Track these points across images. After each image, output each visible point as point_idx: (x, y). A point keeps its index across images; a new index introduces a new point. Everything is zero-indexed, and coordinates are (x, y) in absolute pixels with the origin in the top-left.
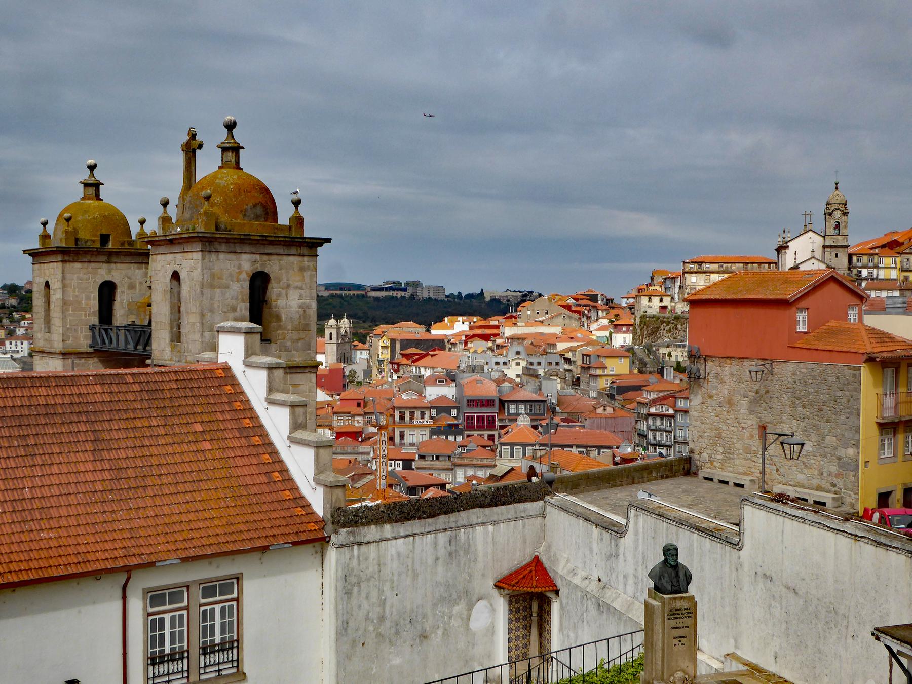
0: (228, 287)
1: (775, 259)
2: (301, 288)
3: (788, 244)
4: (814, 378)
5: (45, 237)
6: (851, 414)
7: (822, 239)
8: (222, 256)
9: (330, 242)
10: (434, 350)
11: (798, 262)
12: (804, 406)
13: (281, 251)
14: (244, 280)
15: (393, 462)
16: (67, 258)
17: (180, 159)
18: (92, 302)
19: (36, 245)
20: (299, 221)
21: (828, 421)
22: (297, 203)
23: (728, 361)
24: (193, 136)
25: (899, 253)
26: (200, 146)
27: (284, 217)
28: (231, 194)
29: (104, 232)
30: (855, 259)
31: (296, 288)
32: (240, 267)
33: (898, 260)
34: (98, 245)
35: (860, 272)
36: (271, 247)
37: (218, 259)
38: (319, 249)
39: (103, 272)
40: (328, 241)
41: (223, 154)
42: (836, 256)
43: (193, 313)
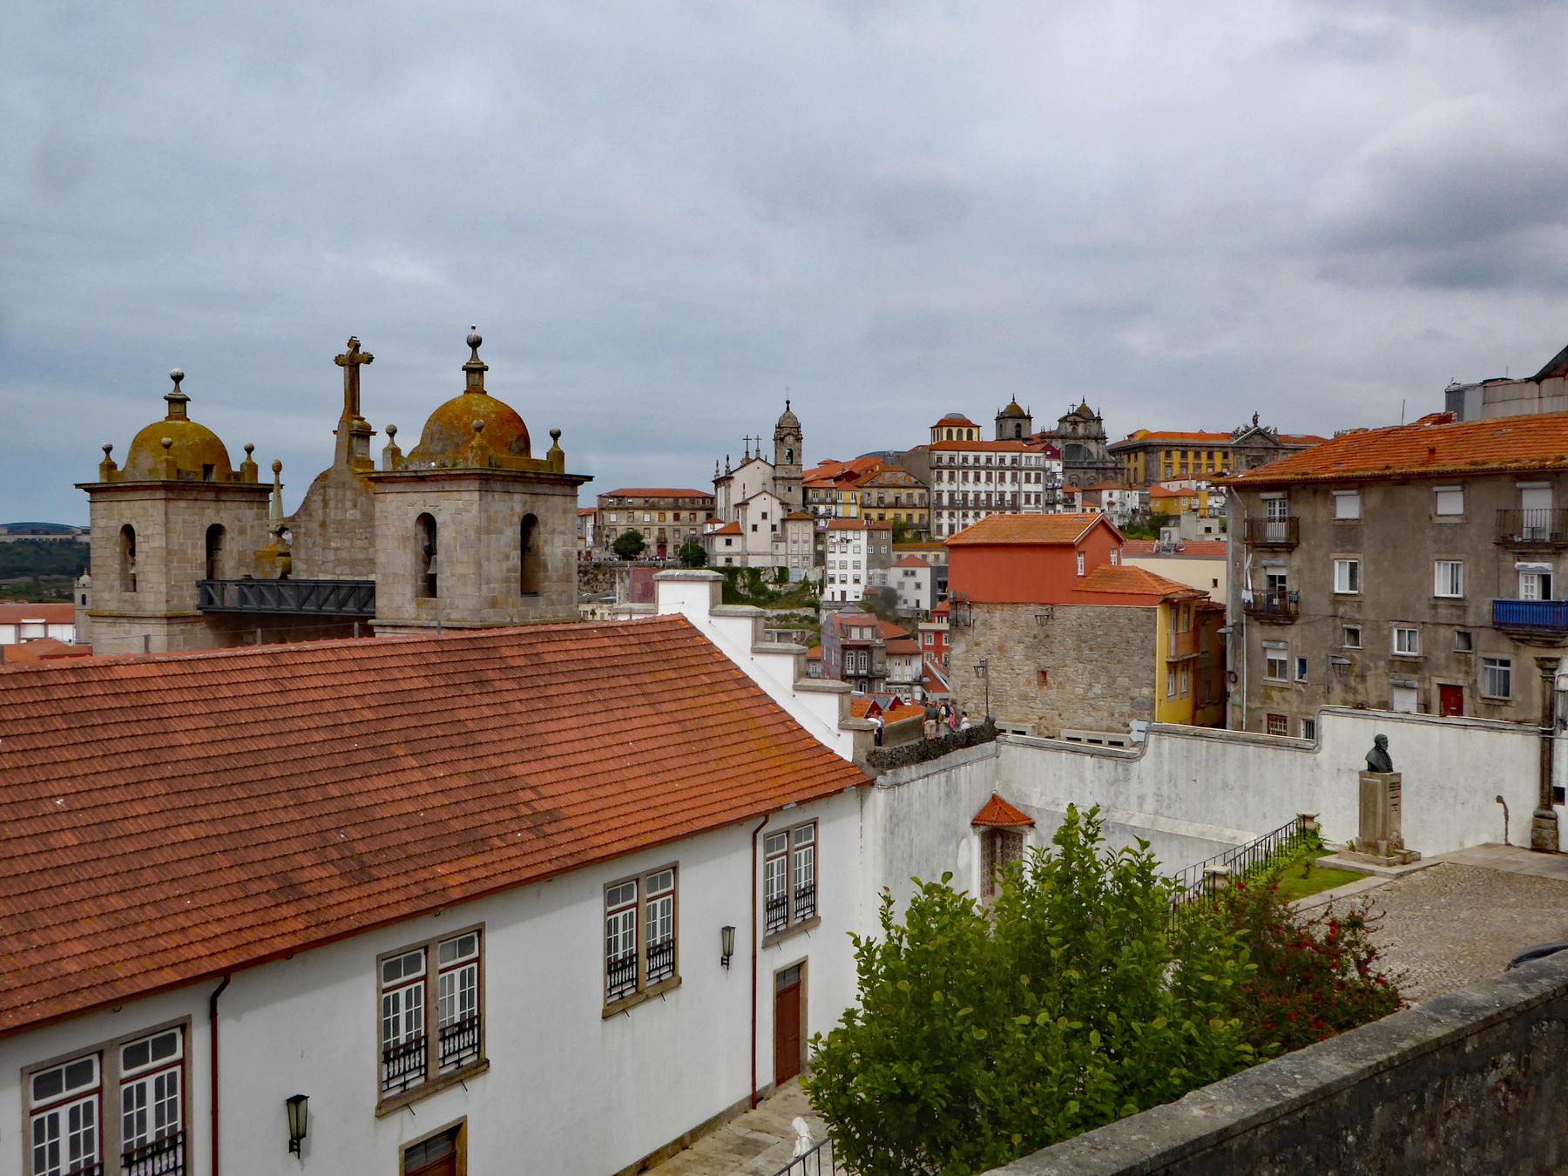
0: (501, 532)
1: (712, 492)
2: (564, 533)
3: (733, 475)
4: (1103, 620)
5: (109, 467)
6: (1145, 654)
7: (771, 469)
8: (497, 496)
11: (747, 497)
12: (1091, 649)
13: (547, 491)
16: (170, 495)
17: (340, 374)
18: (199, 551)
19: (95, 477)
20: (558, 456)
21: (1119, 662)
22: (556, 435)
23: (999, 607)
25: (859, 487)
26: (369, 360)
27: (539, 451)
28: (495, 424)
29: (208, 462)
30: (810, 493)
31: (561, 533)
32: (512, 509)
33: (858, 494)
34: (200, 478)
35: (816, 509)
36: (539, 485)
37: (493, 500)
39: (213, 514)
40: (590, 478)
41: (467, 377)
42: (790, 489)
43: (462, 563)
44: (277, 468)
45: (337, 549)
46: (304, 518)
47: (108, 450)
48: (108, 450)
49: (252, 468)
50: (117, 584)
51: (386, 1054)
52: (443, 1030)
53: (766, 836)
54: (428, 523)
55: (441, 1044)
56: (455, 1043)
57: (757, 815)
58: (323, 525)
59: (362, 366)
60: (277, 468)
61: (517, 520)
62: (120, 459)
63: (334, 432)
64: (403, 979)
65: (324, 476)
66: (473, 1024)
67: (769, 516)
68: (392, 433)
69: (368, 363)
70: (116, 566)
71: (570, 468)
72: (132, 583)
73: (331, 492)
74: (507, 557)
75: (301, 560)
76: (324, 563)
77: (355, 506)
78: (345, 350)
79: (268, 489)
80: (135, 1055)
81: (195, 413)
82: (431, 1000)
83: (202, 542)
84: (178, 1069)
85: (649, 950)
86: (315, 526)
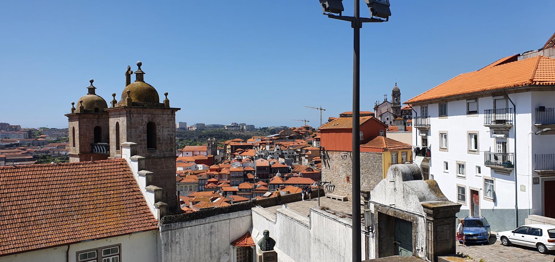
2: (169, 128)
9: (180, 110)
10: (248, 149)
14: (145, 125)
15: (229, 192)
20: (167, 101)
22: (166, 94)
27: (162, 100)
31: (166, 127)
32: (142, 120)
38: (176, 112)
40: (180, 109)
54: (117, 124)
61: (144, 123)
67: (389, 119)
71: (171, 106)
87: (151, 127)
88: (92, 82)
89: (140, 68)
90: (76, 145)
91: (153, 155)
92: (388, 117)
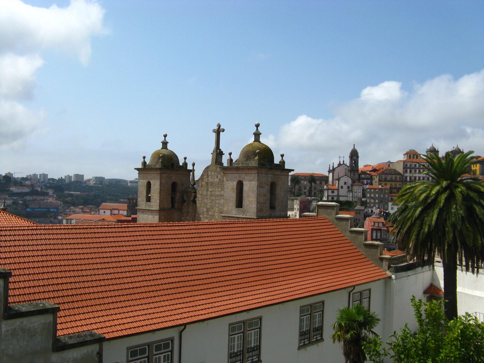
0: (264, 187)
1: (328, 175)
5: (144, 163)
11: (340, 177)
17: (214, 135)
20: (283, 163)
24: (219, 126)
26: (223, 130)
27: (277, 160)
40: (293, 170)
44: (194, 165)
45: (211, 191)
46: (201, 181)
47: (144, 158)
48: (144, 158)
49: (185, 164)
50: (145, 199)
51: (231, 354)
52: (248, 349)
53: (353, 294)
55: (247, 354)
56: (250, 354)
57: (351, 286)
58: (207, 183)
59: (221, 133)
60: (194, 165)
61: (269, 183)
62: (148, 161)
63: (212, 154)
64: (237, 332)
65: (207, 168)
66: (258, 348)
67: (347, 184)
68: (230, 154)
69: (223, 132)
70: (145, 193)
71: (286, 167)
72: (148, 199)
73: (209, 173)
74: (265, 196)
75: (200, 194)
76: (207, 195)
77: (217, 177)
78: (216, 128)
79: (190, 171)
80: (158, 348)
81: (169, 147)
82: (245, 339)
83: (170, 187)
84: (170, 353)
85: (314, 329)
86: (204, 183)
87: (273, 186)
88: (165, 136)
89: (257, 129)
90: (245, 202)
91: (273, 214)
92: (346, 181)
